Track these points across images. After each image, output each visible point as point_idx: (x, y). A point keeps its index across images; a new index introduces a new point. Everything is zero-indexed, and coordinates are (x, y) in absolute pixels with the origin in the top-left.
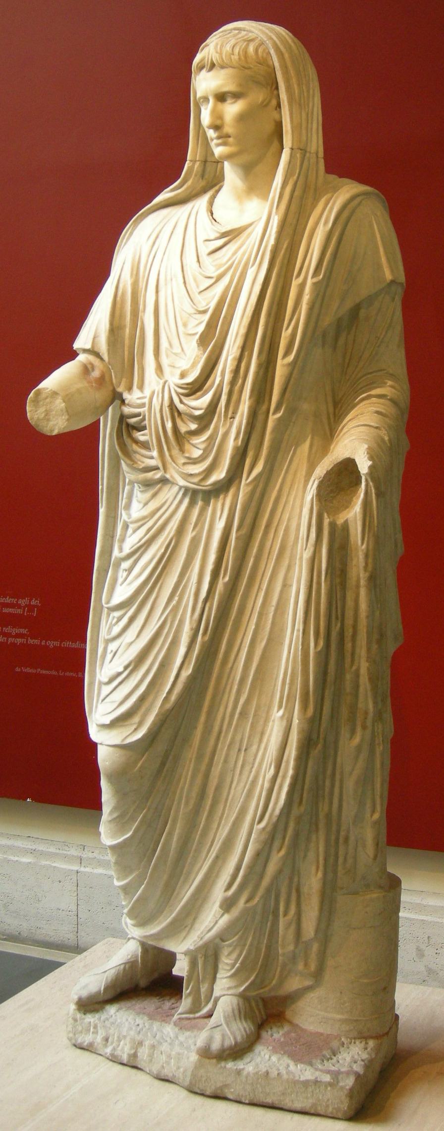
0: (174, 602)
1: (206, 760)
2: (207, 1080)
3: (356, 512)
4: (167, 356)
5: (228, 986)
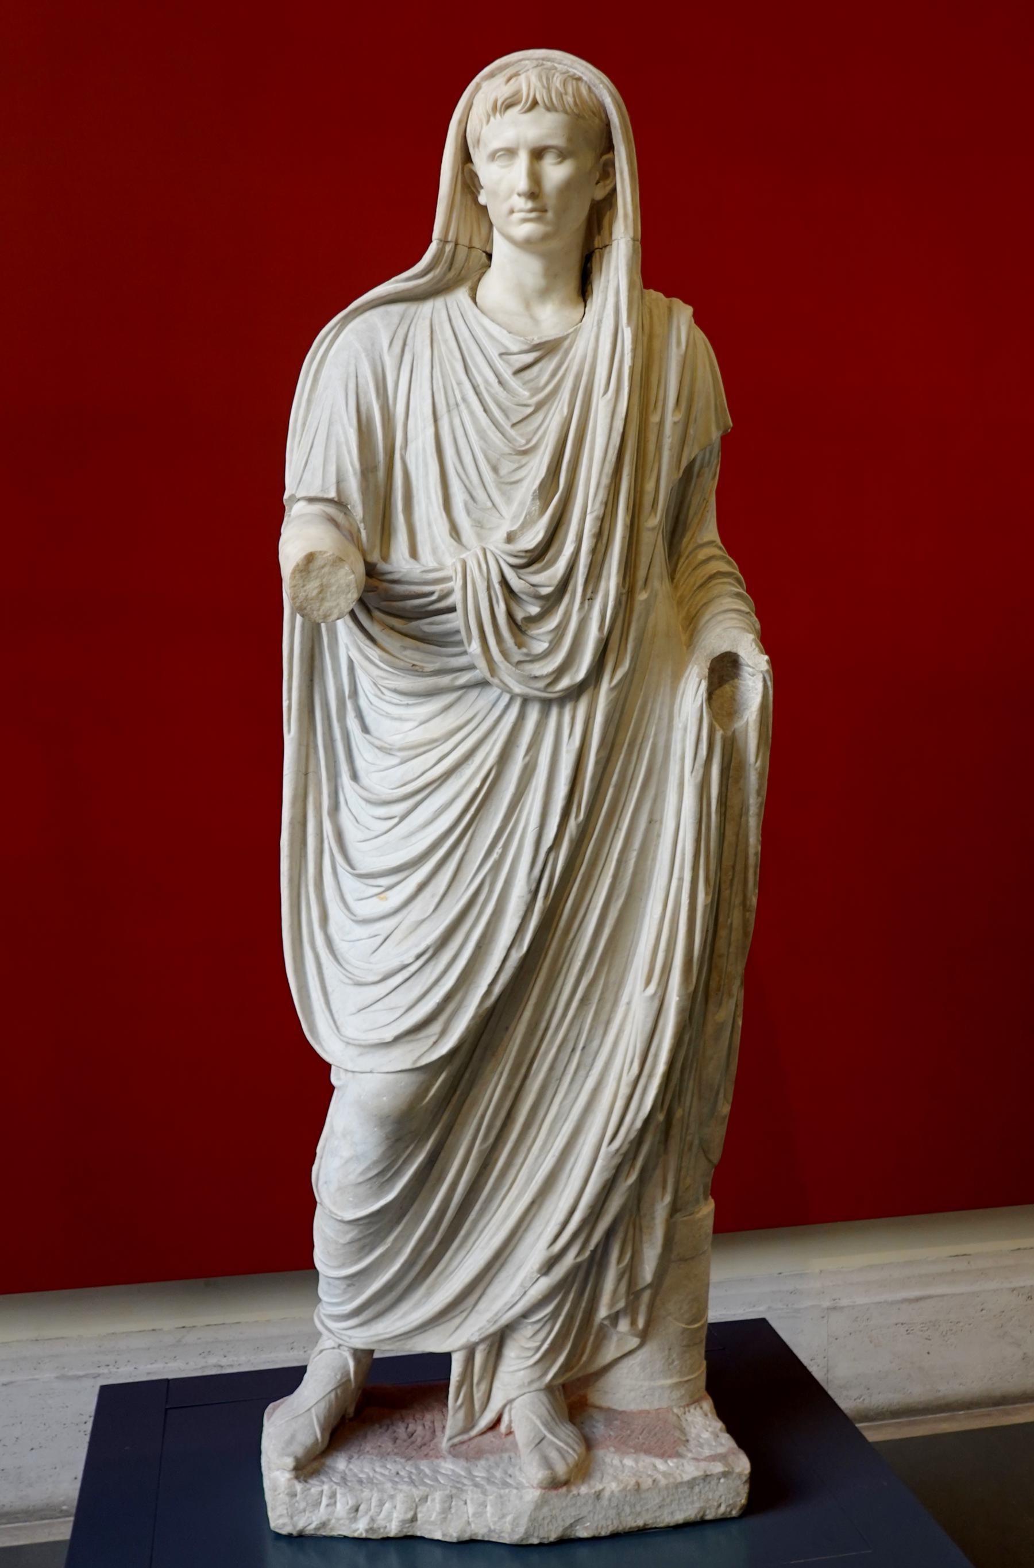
0: (495, 856)
1: (523, 1071)
2: (551, 1521)
3: (747, 723)
4: (468, 512)
5: (527, 1381)
